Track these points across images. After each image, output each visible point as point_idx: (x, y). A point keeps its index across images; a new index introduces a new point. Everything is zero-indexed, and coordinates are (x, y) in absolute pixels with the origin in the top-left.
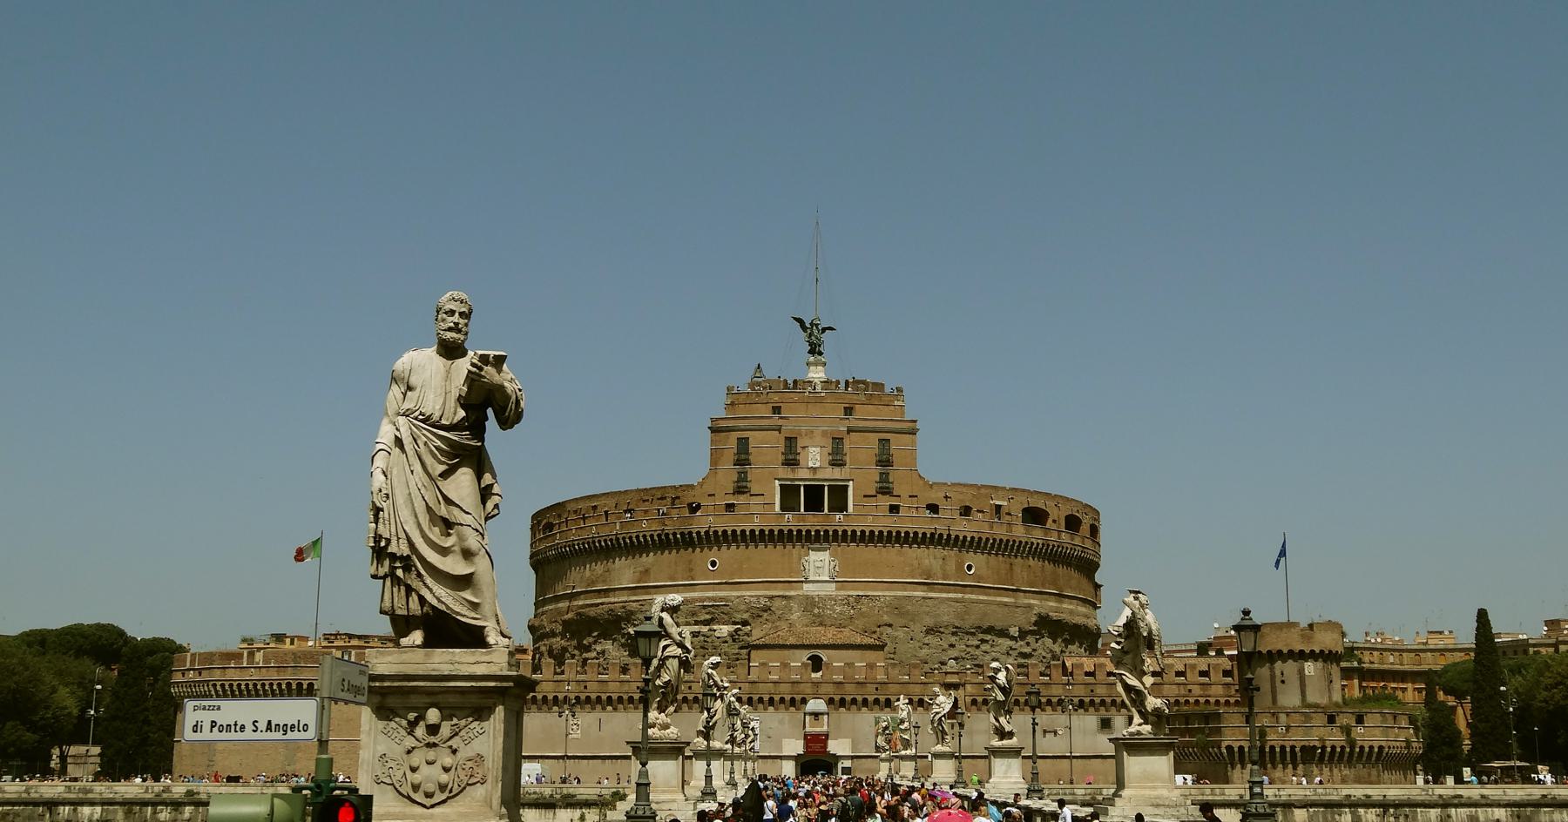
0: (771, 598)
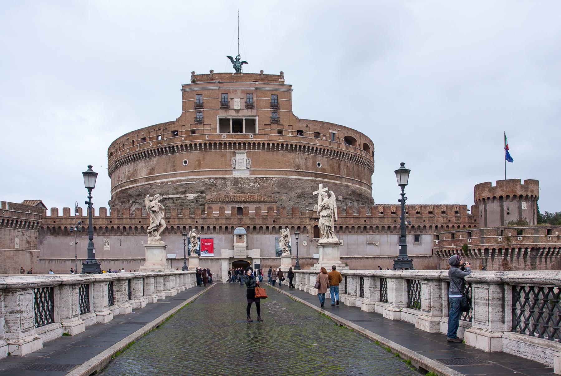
0: (216, 179)
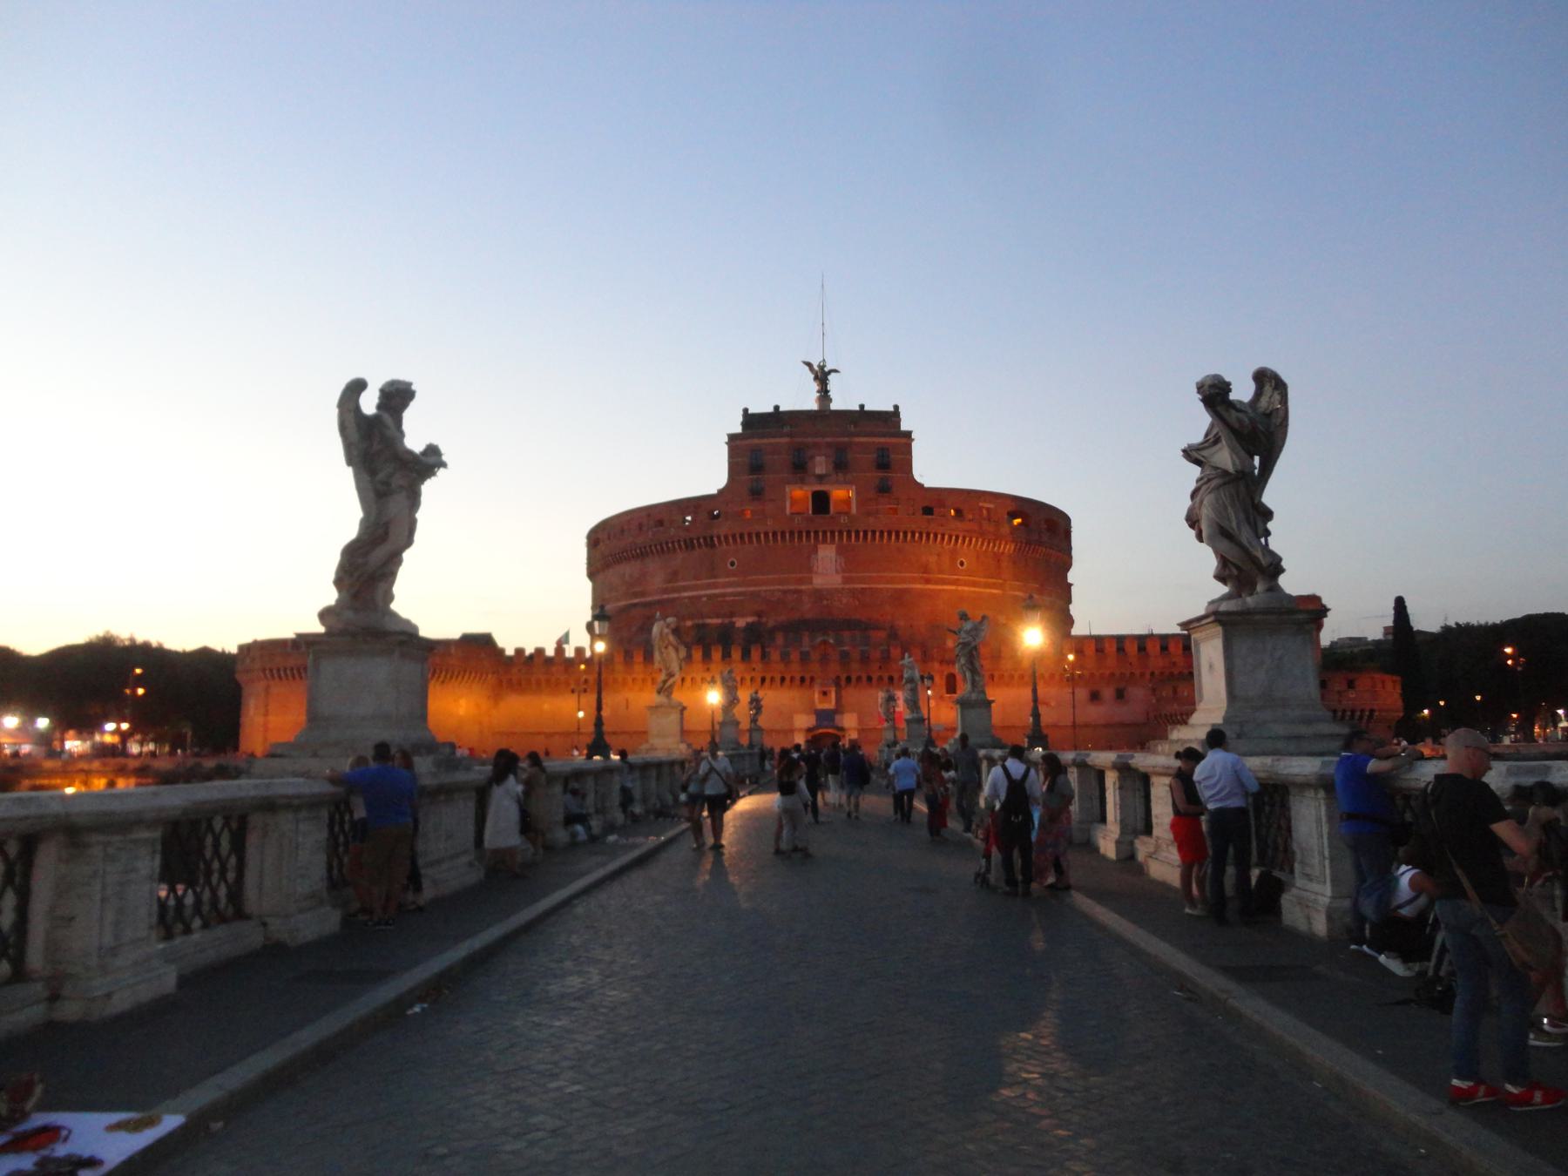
0: (785, 592)
